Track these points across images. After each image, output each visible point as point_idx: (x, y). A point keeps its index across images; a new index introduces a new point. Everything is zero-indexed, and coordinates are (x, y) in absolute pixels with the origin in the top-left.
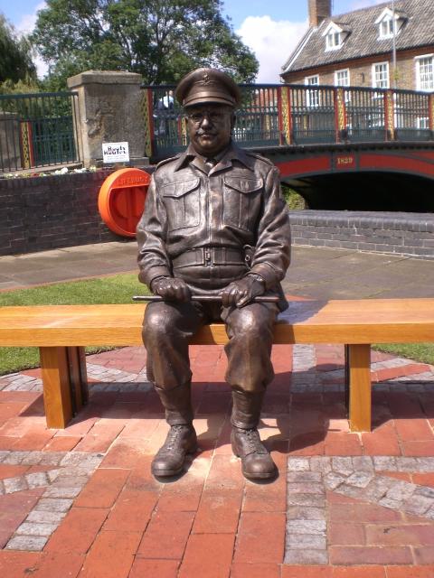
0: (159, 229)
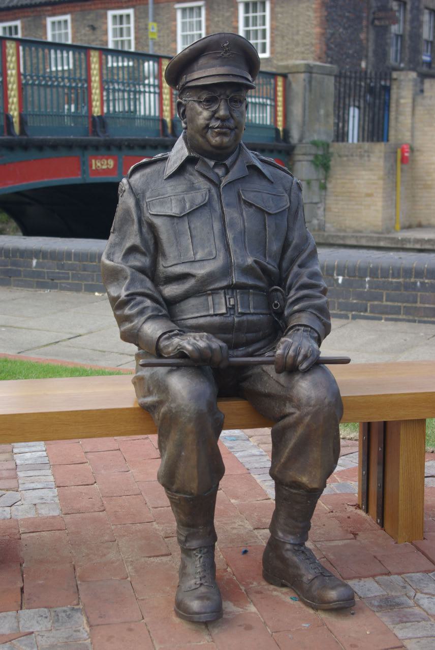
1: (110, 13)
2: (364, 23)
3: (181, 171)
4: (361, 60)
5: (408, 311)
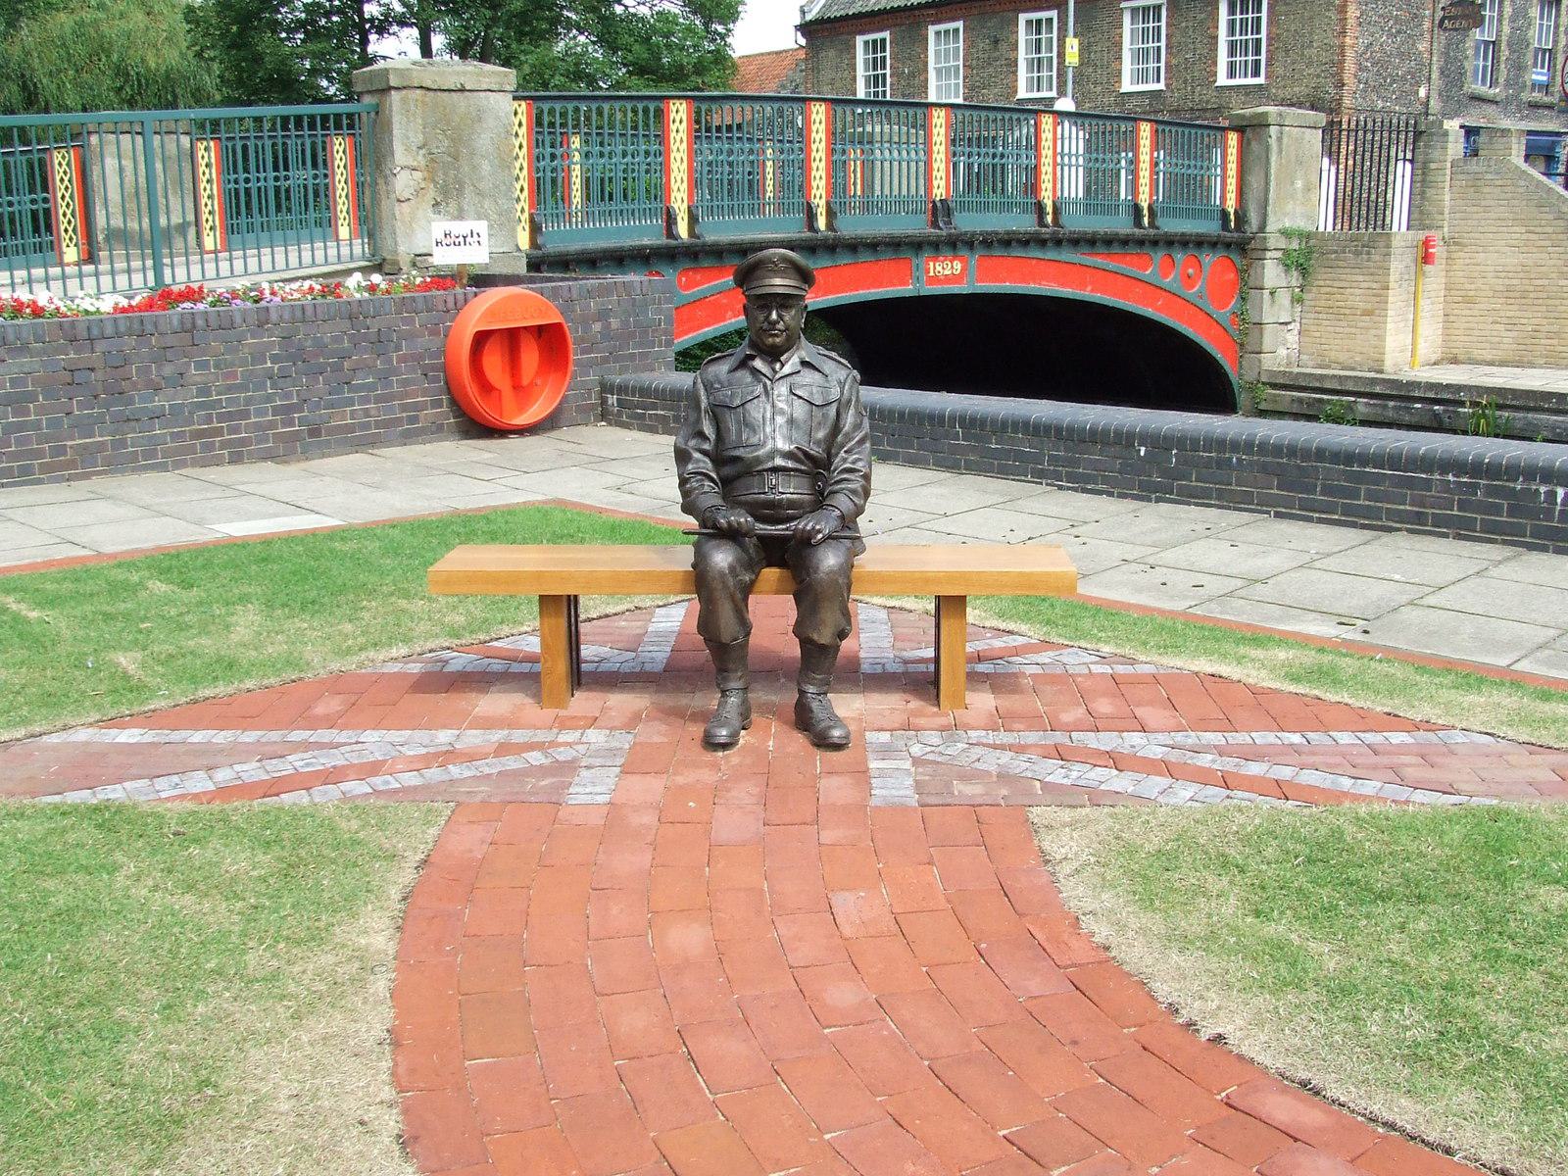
1: (1023, 18)
5: (1220, 495)
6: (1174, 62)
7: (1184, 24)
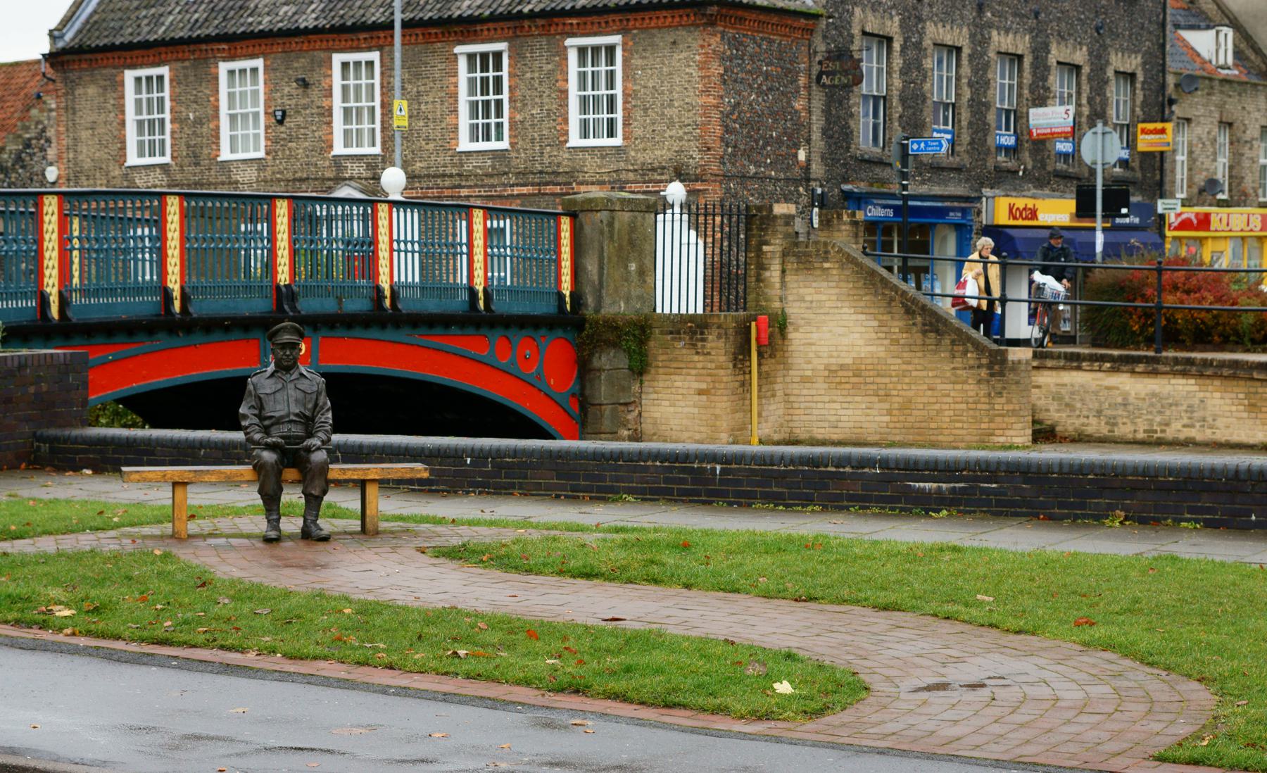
0: (256, 412)
1: (337, 59)
2: (802, 81)
3: (272, 375)
4: (797, 147)
6: (518, 117)
7: (528, 75)
